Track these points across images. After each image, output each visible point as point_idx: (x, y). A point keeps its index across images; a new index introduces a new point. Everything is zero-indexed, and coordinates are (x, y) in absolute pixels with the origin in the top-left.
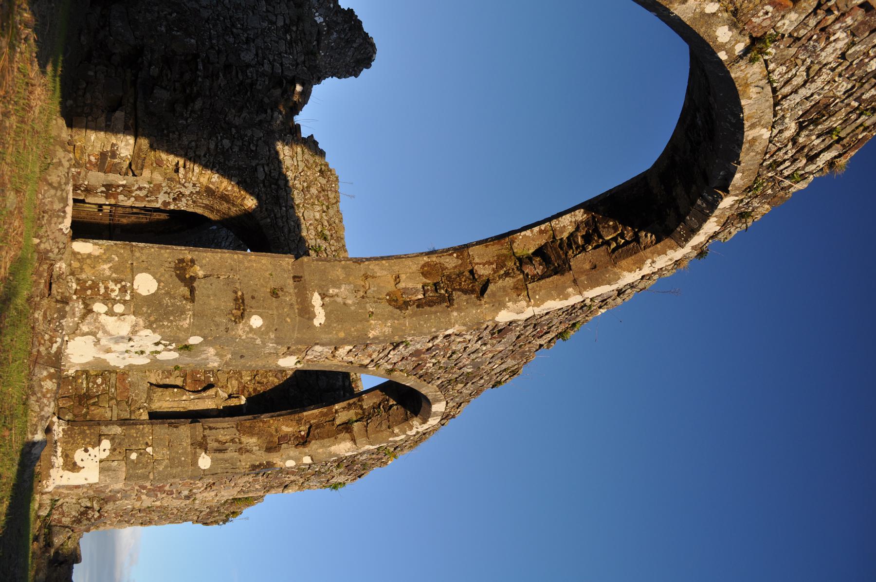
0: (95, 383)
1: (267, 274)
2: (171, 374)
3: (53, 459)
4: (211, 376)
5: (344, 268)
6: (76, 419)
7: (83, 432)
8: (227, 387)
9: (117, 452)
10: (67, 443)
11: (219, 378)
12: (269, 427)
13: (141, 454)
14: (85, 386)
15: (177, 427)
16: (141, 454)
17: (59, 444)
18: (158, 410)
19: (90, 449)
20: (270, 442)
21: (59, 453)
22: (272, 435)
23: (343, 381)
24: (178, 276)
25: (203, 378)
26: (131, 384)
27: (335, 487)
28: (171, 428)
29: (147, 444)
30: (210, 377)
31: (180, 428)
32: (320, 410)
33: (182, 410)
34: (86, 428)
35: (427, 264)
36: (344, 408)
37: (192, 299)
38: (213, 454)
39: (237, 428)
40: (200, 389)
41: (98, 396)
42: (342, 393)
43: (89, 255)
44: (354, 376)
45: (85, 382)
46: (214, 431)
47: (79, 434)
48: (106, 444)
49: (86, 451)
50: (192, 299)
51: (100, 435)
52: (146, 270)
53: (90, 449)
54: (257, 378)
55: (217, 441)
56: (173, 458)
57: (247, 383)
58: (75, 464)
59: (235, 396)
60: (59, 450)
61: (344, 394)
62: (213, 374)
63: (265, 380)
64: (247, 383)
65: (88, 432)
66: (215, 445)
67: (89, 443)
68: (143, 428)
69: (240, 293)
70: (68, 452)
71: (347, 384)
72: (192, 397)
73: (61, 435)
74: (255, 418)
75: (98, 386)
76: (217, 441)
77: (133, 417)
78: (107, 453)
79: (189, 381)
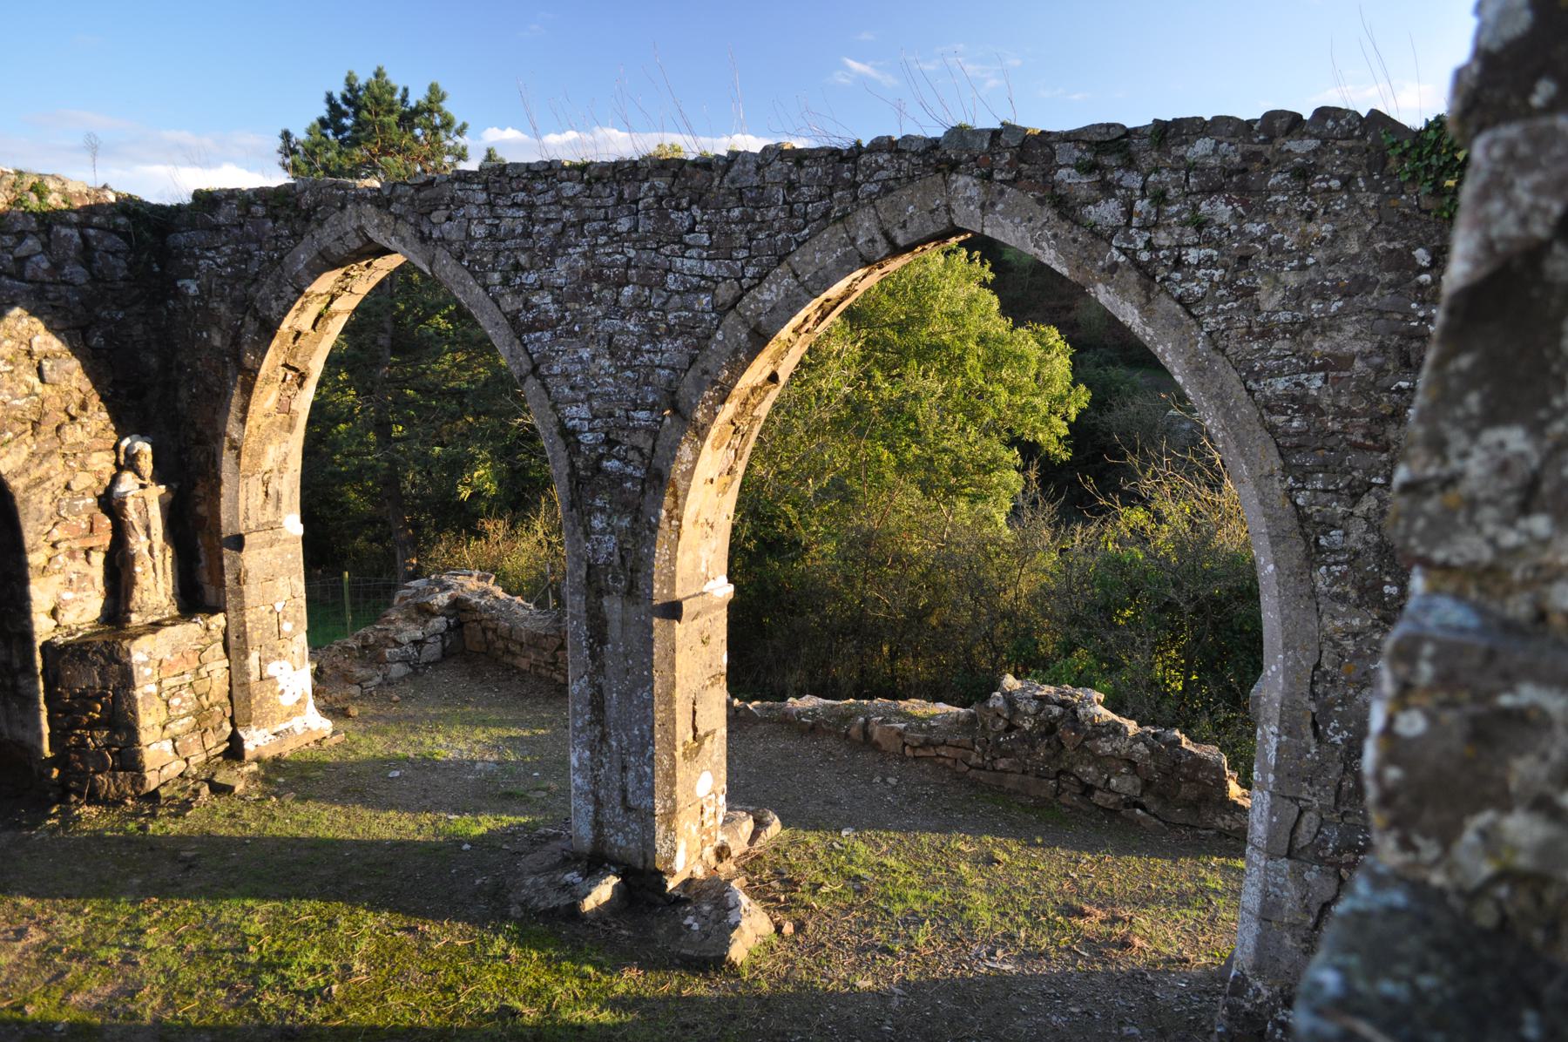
0: (179, 707)
1: (691, 653)
2: (86, 575)
3: (299, 730)
4: (82, 502)
5: (684, 553)
6: (229, 714)
7: (259, 704)
8: (100, 472)
9: (281, 650)
10: (273, 719)
11: (84, 486)
12: (259, 427)
13: (285, 618)
14: (186, 720)
15: (246, 572)
16: (285, 618)
17: (275, 731)
18: (170, 592)
19: (279, 689)
20: (281, 427)
21: (287, 725)
22: (272, 423)
23: (69, 224)
24: (697, 755)
25: (85, 517)
26: (174, 651)
27: (55, 178)
28: (248, 581)
29: (271, 612)
30: (85, 505)
31: (247, 567)
32: (271, 349)
33: (169, 553)
34: (253, 702)
35: (713, 446)
36: (297, 316)
37: (714, 732)
38: (283, 512)
39: (248, 477)
40: (109, 521)
41: (198, 697)
42: (92, 232)
43: (687, 850)
44: (55, 195)
45: (181, 722)
46: (250, 513)
47: (261, 707)
48: (272, 669)
49: (282, 692)
50: (714, 732)
51: (261, 679)
52: (693, 789)
53: (279, 689)
54: (73, 413)
55: (263, 507)
56: (289, 570)
57: (89, 433)
58: (299, 702)
59: (122, 457)
60: (281, 727)
61: (93, 228)
62: (79, 499)
63: (77, 396)
64: (89, 433)
65: (258, 697)
66: (270, 508)
67: (272, 691)
68: (251, 621)
69: (708, 683)
70: (285, 714)
71: (75, 218)
72: (143, 538)
73: (264, 731)
74: (236, 447)
75: (184, 700)
76: (263, 507)
77: (220, 636)
78: (285, 664)
79: (94, 542)
